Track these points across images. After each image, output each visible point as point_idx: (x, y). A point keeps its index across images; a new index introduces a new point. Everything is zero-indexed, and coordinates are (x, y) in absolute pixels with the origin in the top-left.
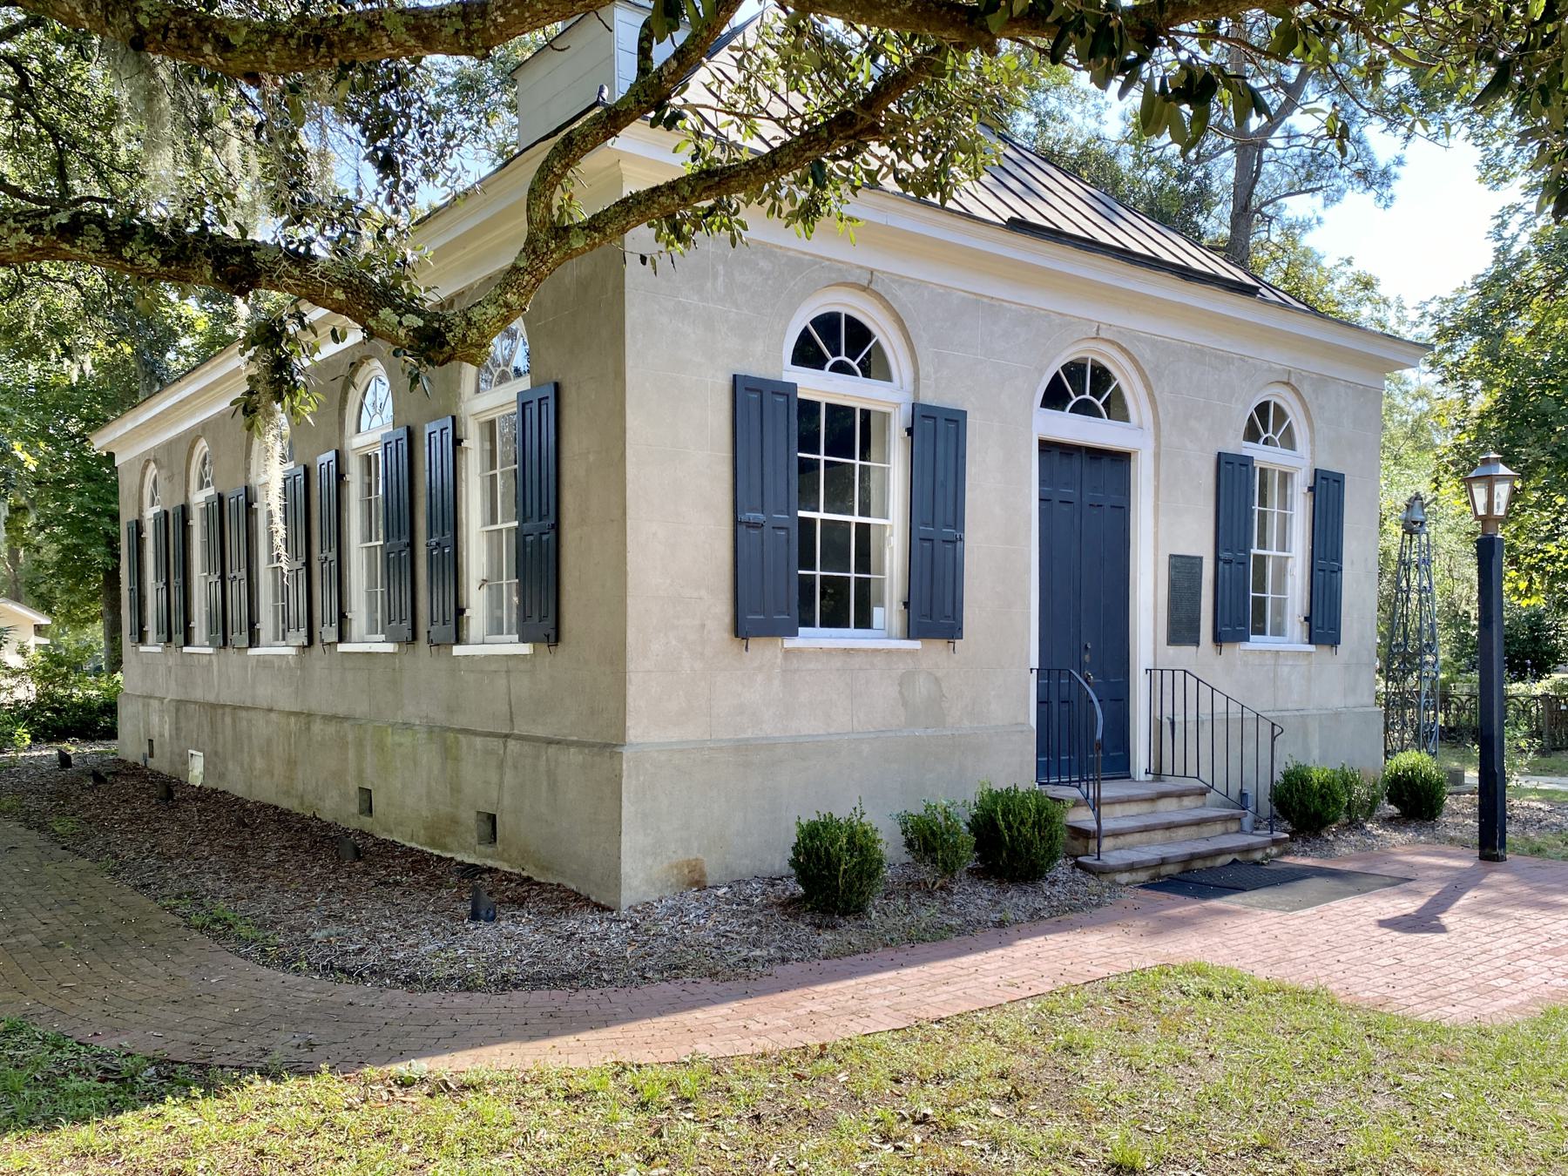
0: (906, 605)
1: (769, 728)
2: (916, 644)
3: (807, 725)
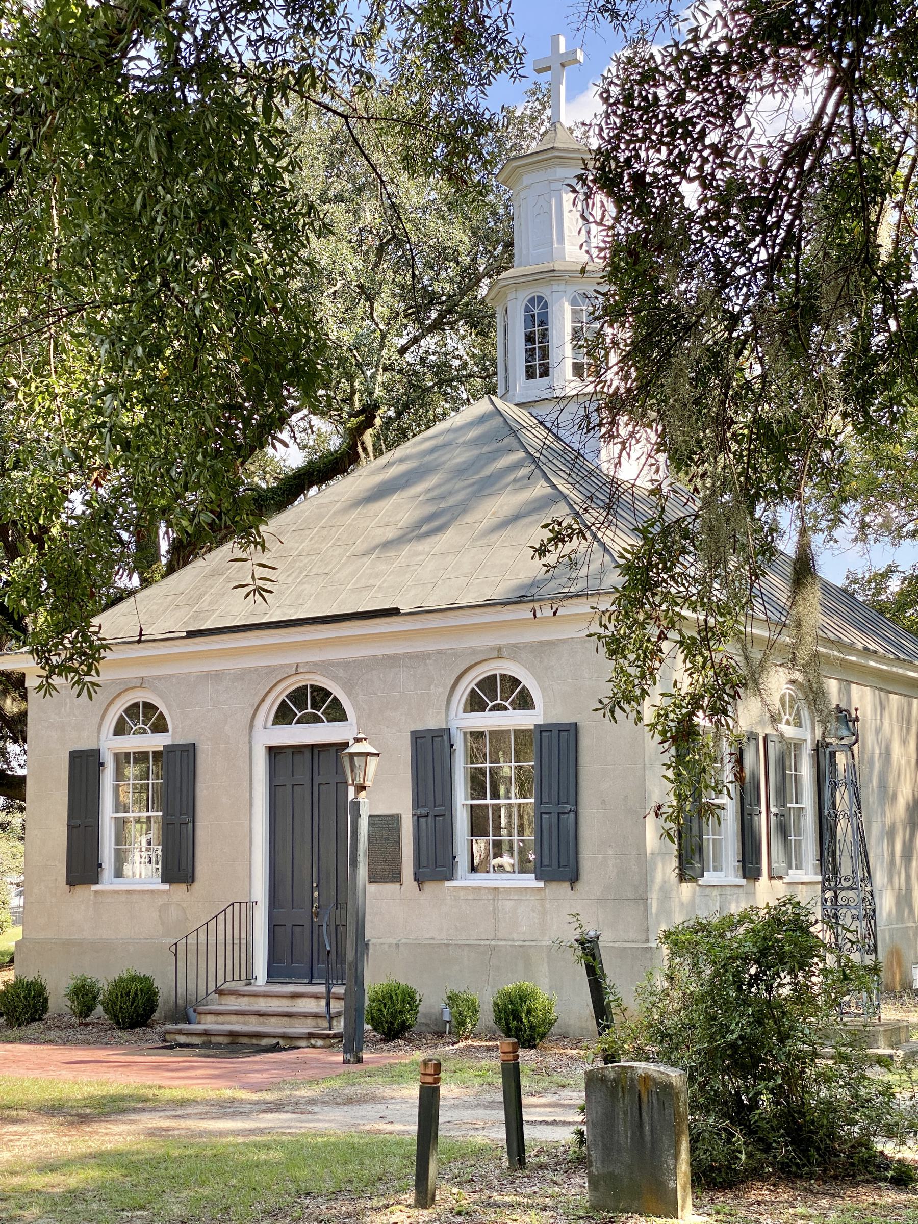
0: (100, 866)
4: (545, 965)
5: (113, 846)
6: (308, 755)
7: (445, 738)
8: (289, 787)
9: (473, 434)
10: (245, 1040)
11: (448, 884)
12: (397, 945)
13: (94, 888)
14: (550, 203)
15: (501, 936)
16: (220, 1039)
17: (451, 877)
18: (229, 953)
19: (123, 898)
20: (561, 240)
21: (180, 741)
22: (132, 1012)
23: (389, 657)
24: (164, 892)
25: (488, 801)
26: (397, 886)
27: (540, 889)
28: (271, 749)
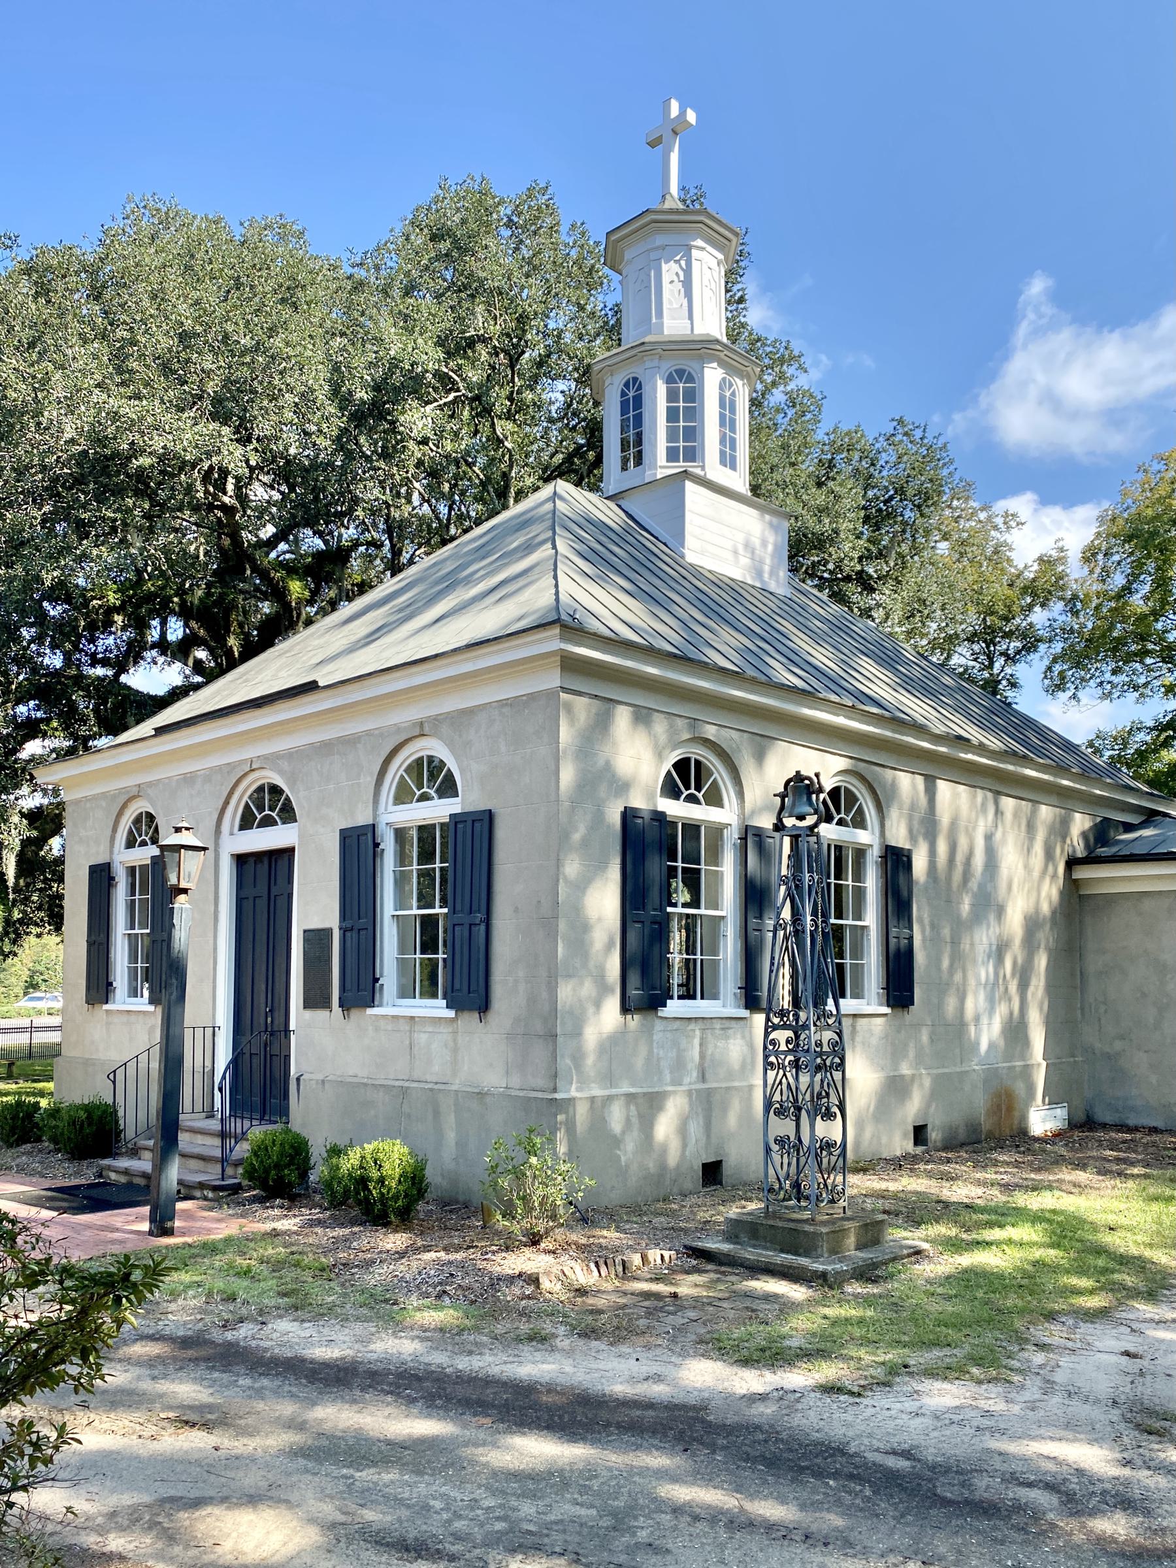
4: (453, 1116)
5: (126, 964)
7: (370, 835)
8: (251, 900)
11: (370, 1011)
12: (323, 1081)
14: (649, 276)
17: (371, 1003)
19: (124, 1018)
20: (660, 314)
27: (452, 1020)
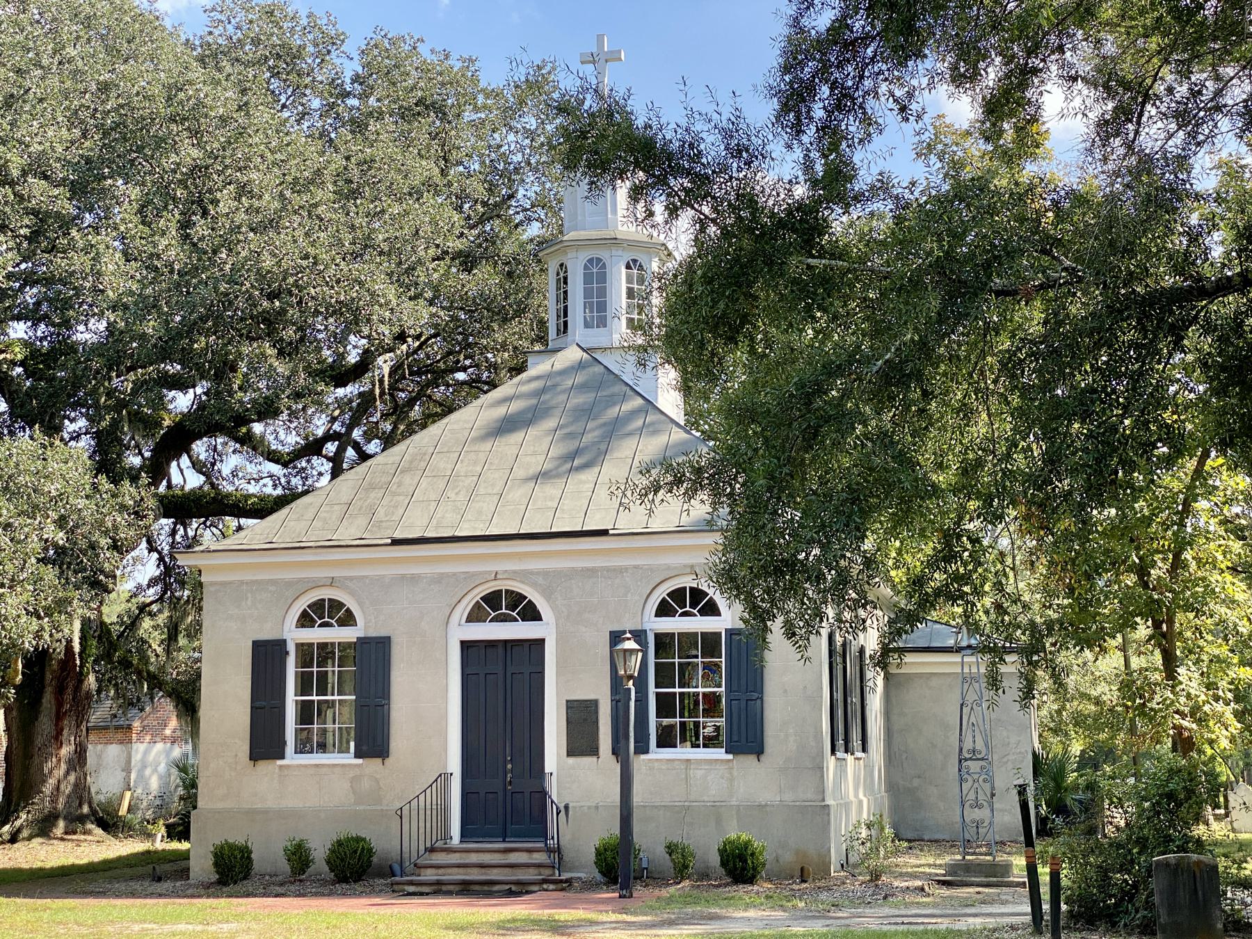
1: (271, 803)
2: (360, 761)
3: (291, 803)
6: (501, 650)
9: (580, 378)
10: (477, 888)
12: (597, 807)
13: (279, 762)
15: (692, 798)
16: (451, 888)
18: (428, 818)
21: (372, 633)
22: (354, 868)
23: (588, 569)
24: (356, 765)
25: (677, 690)
26: (595, 759)
27: (729, 761)
28: (462, 642)
